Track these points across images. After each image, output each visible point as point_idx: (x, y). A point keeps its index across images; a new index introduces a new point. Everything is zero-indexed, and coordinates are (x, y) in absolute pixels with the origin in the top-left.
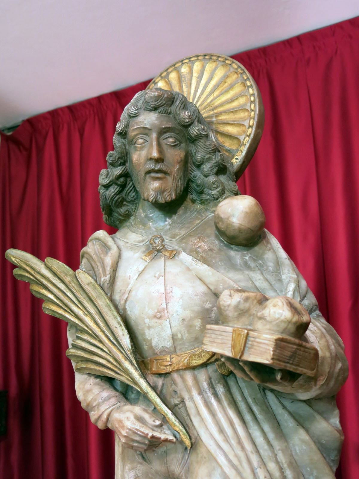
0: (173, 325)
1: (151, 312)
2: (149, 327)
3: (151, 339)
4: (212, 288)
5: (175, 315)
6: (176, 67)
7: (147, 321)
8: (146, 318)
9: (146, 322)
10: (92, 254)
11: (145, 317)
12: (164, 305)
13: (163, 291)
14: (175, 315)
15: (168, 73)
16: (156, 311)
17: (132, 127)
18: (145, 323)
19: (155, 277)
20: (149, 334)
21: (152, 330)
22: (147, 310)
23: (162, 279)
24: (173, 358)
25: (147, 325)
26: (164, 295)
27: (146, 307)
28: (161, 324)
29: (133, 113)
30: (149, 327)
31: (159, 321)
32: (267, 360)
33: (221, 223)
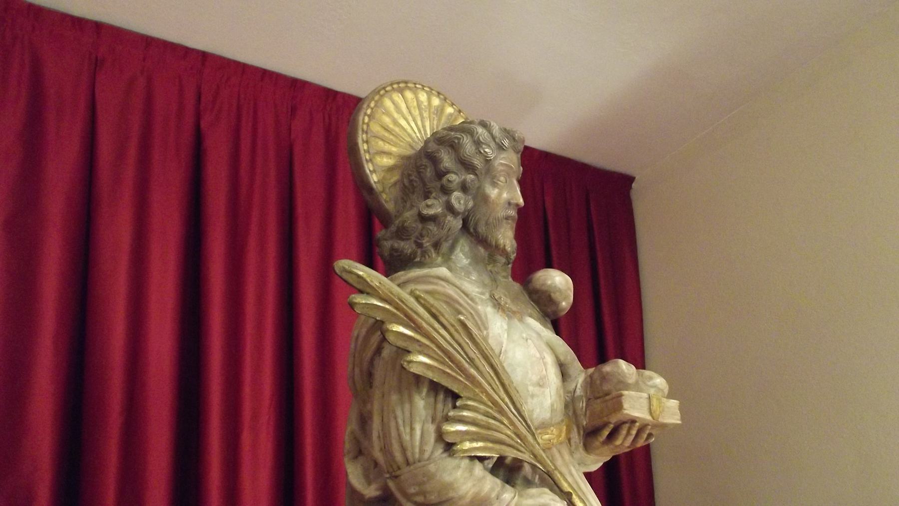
0: (552, 394)
1: (535, 378)
2: (533, 396)
3: (533, 410)
4: (562, 358)
5: (553, 383)
6: (409, 87)
7: (531, 388)
8: (530, 385)
9: (529, 390)
10: (456, 296)
11: (529, 383)
12: (544, 372)
13: (538, 355)
14: (553, 383)
15: (399, 87)
16: (539, 377)
17: (501, 160)
18: (528, 391)
19: (523, 338)
20: (532, 403)
21: (535, 400)
22: (530, 375)
23: (529, 341)
24: (552, 431)
25: (531, 393)
26: (541, 360)
27: (530, 372)
28: (544, 392)
29: (506, 146)
30: (533, 396)
31: (542, 389)
32: (678, 420)
33: (558, 294)
